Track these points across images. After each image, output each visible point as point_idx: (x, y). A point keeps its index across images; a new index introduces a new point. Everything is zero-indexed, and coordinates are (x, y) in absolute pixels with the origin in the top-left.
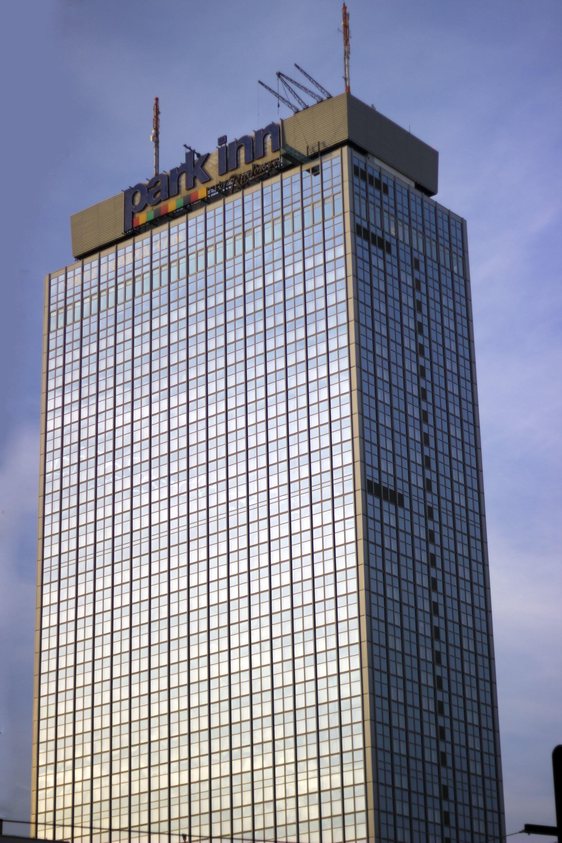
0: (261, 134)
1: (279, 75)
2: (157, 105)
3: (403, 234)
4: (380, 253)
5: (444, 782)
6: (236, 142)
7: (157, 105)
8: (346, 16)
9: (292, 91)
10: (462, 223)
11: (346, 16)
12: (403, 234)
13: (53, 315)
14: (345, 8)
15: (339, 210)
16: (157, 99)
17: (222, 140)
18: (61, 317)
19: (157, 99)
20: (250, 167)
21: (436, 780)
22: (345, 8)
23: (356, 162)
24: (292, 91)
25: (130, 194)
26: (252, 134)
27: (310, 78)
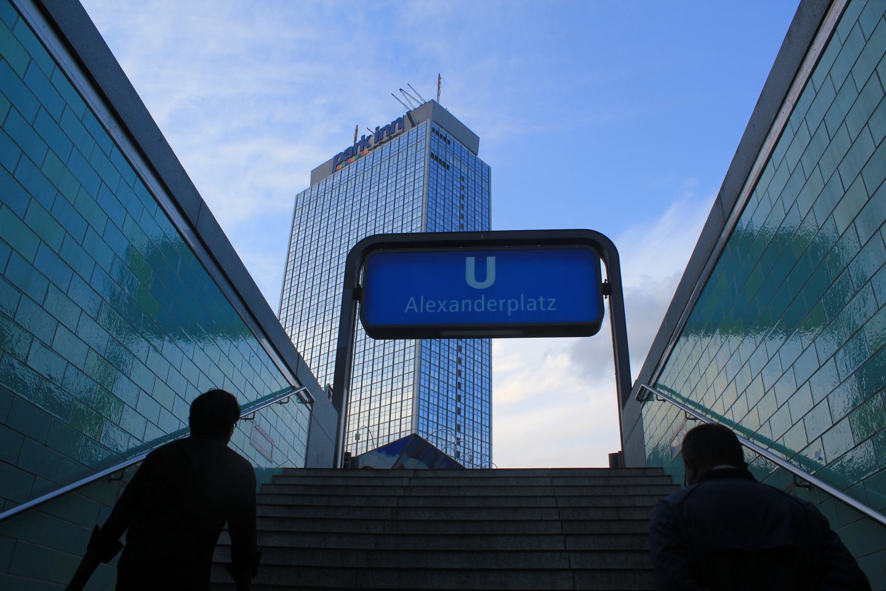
0: (394, 123)
1: (401, 89)
2: (357, 128)
3: (457, 164)
4: (444, 168)
5: (458, 423)
6: (383, 128)
7: (357, 128)
8: (439, 78)
9: (408, 100)
10: (489, 169)
11: (439, 78)
12: (457, 164)
13: (297, 211)
14: (439, 75)
15: (423, 146)
16: (357, 126)
17: (377, 128)
18: (300, 212)
19: (357, 126)
20: (388, 138)
21: (454, 421)
22: (439, 75)
23: (433, 126)
24: (408, 100)
25: (337, 157)
26: (390, 123)
27: (417, 94)
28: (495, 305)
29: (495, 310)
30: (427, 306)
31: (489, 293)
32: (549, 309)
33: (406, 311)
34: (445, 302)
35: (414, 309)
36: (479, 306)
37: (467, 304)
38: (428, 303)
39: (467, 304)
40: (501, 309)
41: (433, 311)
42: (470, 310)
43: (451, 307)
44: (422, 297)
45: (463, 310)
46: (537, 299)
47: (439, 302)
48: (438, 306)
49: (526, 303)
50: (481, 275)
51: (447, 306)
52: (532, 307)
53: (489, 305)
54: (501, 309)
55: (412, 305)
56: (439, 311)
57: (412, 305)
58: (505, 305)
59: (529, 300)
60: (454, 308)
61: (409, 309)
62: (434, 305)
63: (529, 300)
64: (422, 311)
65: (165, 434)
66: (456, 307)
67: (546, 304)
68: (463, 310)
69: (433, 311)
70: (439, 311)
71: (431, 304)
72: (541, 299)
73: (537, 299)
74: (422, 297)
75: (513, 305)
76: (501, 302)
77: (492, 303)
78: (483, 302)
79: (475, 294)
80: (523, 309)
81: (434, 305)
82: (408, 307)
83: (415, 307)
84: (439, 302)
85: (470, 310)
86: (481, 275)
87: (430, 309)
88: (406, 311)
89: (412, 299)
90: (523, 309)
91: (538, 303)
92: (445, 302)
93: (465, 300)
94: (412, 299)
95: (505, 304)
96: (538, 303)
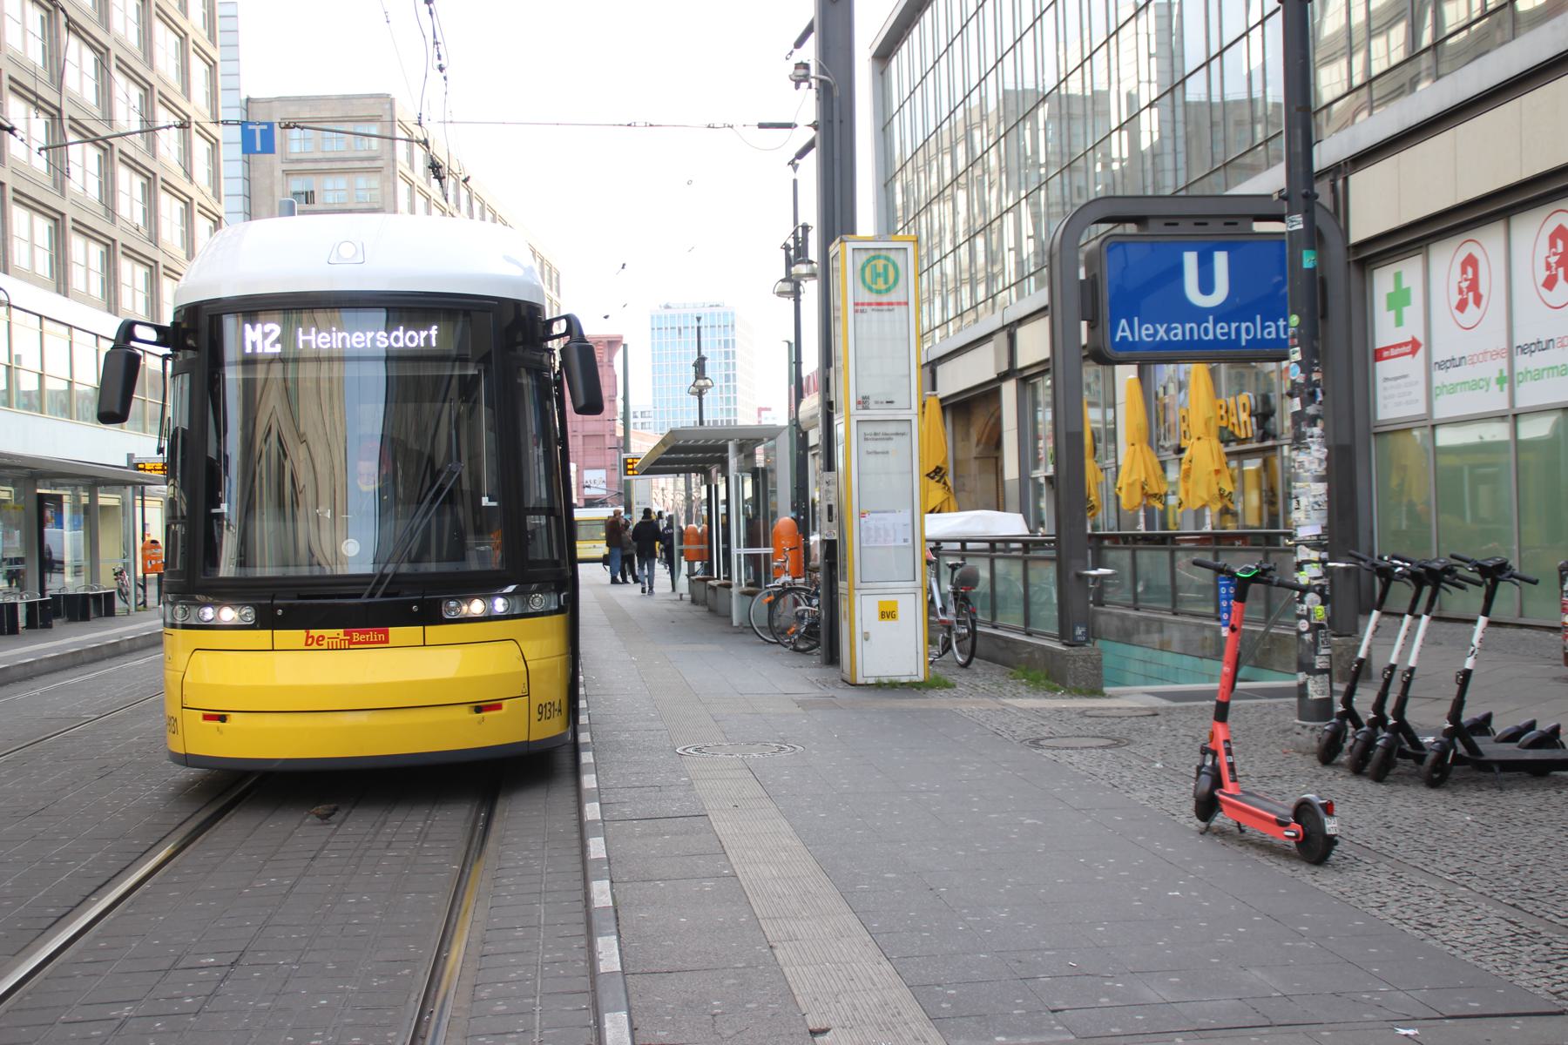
28: (1226, 330)
29: (1225, 338)
30: (1144, 332)
31: (1222, 314)
34: (1165, 326)
36: (1206, 330)
37: (1191, 330)
39: (1191, 330)
40: (1233, 337)
41: (1151, 339)
42: (1196, 338)
43: (1172, 333)
44: (1136, 319)
45: (1188, 338)
46: (1275, 321)
47: (1158, 326)
48: (1156, 332)
49: (1263, 328)
50: (1206, 286)
51: (1167, 331)
52: (1269, 333)
53: (1218, 331)
54: (1233, 337)
56: (1158, 339)
57: (1123, 331)
58: (1238, 330)
59: (1267, 324)
60: (1176, 335)
61: (1121, 337)
62: (1151, 331)
63: (1267, 324)
64: (1137, 339)
65: (812, 156)
66: (1179, 332)
68: (1188, 338)
69: (1151, 339)
70: (1158, 339)
73: (1275, 321)
74: (1136, 319)
75: (1248, 329)
76: (1234, 325)
77: (1222, 328)
78: (1210, 326)
79: (1199, 315)
80: (1259, 337)
81: (1151, 331)
82: (1119, 334)
83: (1128, 333)
84: (1158, 326)
85: (1196, 338)
86: (1206, 286)
87: (1148, 336)
89: (1123, 322)
90: (1259, 337)
91: (1277, 328)
92: (1165, 326)
93: (1189, 323)
94: (1123, 322)
95: (1238, 330)
96: (1277, 328)
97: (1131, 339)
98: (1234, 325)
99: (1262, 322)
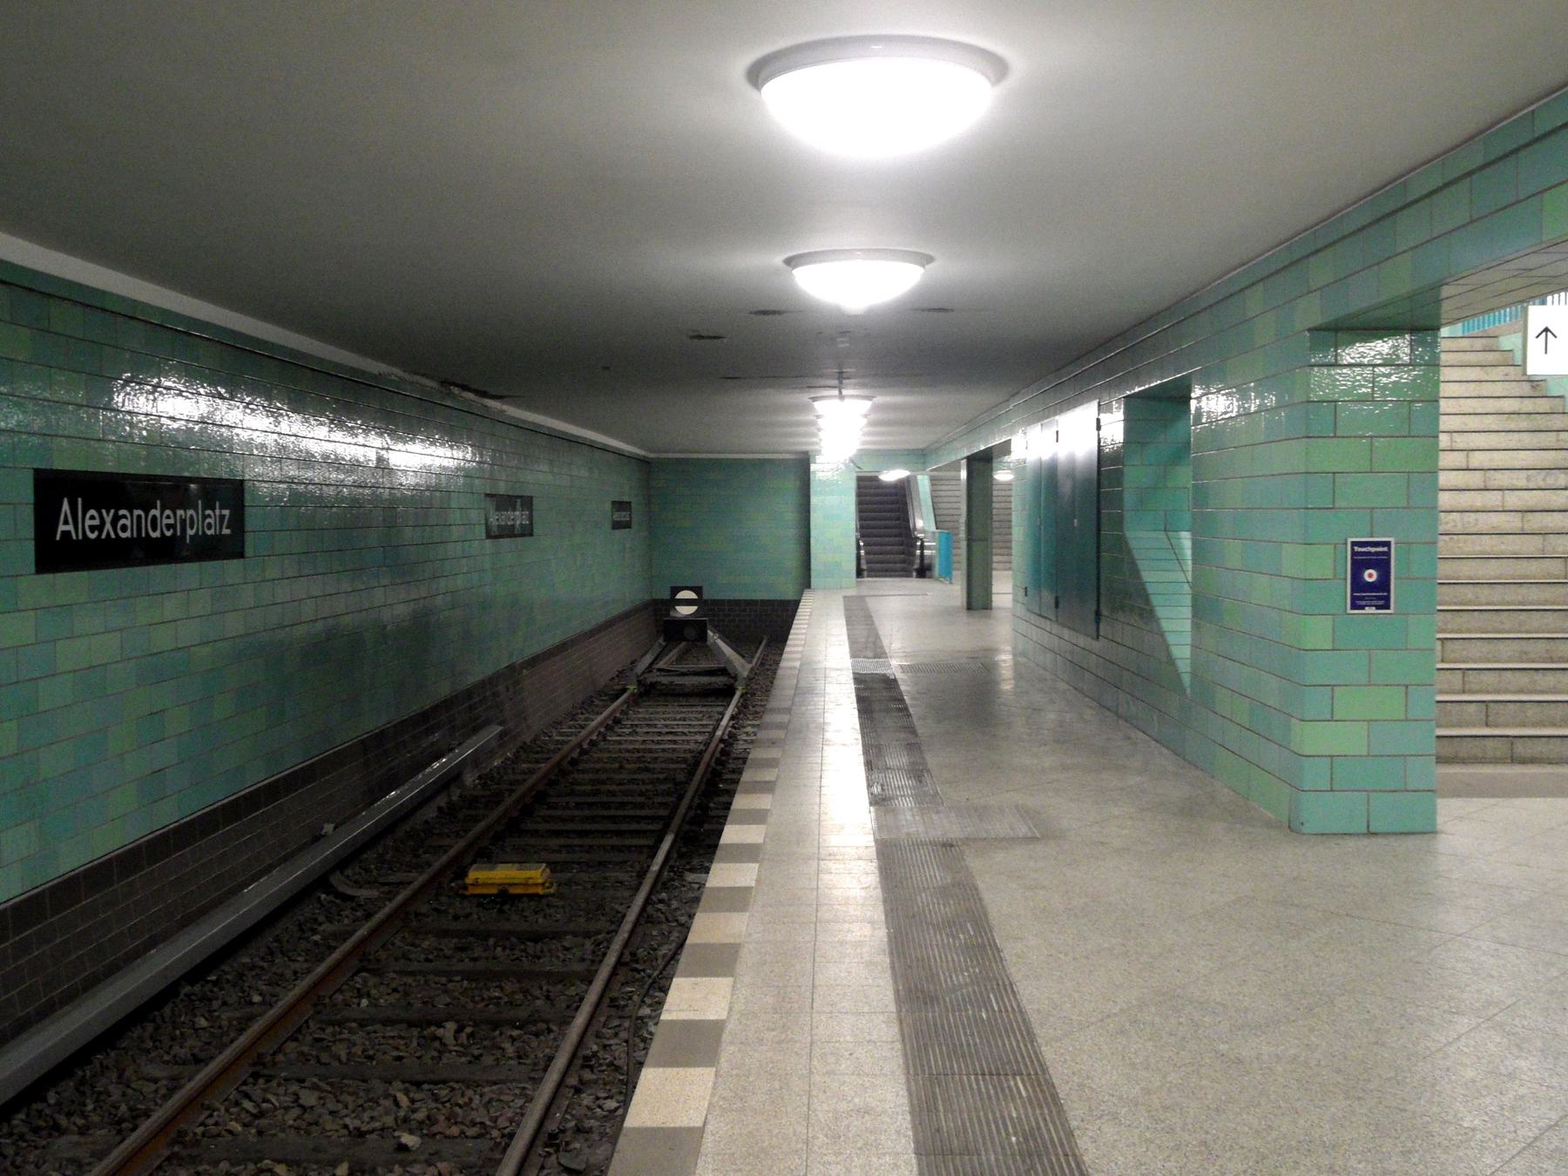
28: (171, 521)
32: (226, 531)
33: (58, 538)
34: (112, 511)
35: (69, 532)
38: (88, 516)
40: (179, 534)
42: (143, 535)
44: (80, 500)
46: (213, 509)
48: (103, 522)
55: (66, 522)
58: (183, 522)
61: (63, 532)
62: (96, 522)
64: (80, 537)
67: (222, 517)
71: (92, 518)
72: (217, 512)
73: (213, 509)
74: (80, 500)
77: (168, 517)
82: (62, 528)
83: (70, 527)
85: (143, 535)
87: (92, 529)
88: (58, 538)
97: (74, 537)
98: (180, 512)
99: (203, 512)
